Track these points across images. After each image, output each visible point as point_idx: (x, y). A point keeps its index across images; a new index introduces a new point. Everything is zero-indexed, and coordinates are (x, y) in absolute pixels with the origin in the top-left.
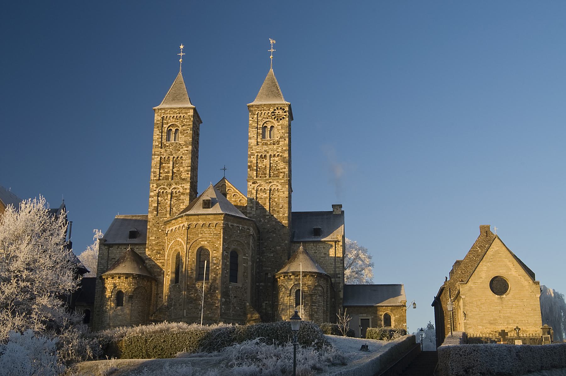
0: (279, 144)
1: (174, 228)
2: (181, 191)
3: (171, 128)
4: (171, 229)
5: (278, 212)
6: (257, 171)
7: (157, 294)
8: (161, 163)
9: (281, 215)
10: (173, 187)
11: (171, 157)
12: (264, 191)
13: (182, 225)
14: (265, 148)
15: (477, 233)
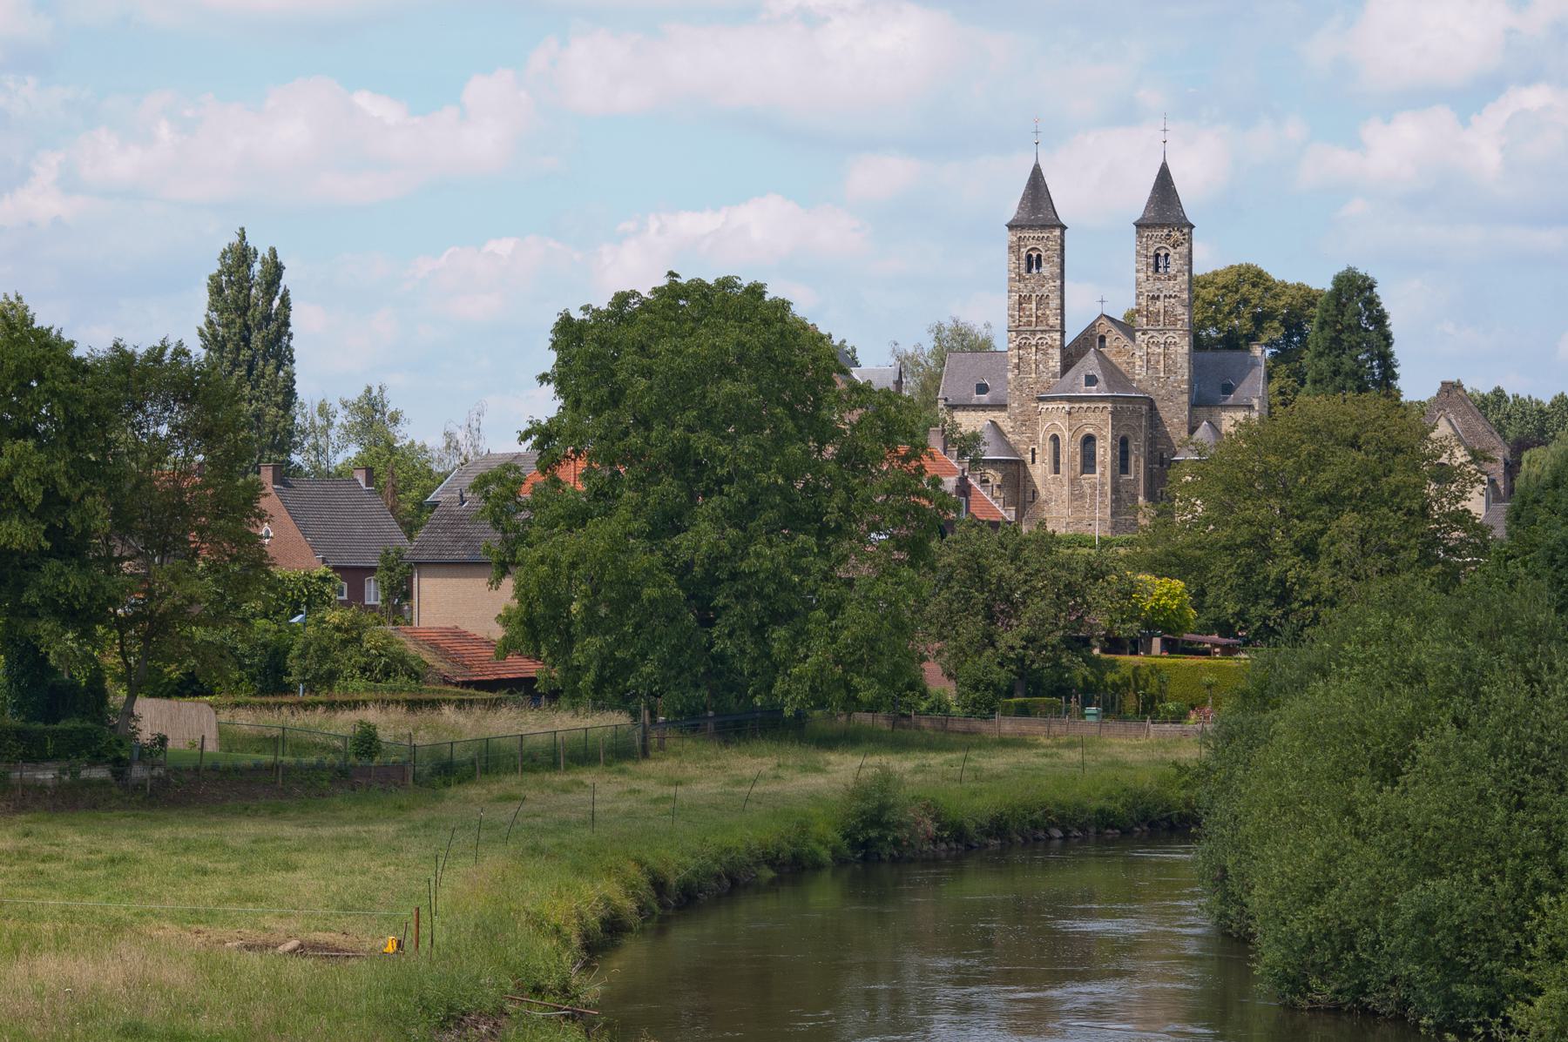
1: (1050, 407)
4: (1045, 407)
6: (1147, 317)
7: (1025, 477)
8: (1020, 304)
9: (1179, 377)
10: (1039, 336)
11: (1034, 295)
13: (1061, 406)
14: (1159, 285)
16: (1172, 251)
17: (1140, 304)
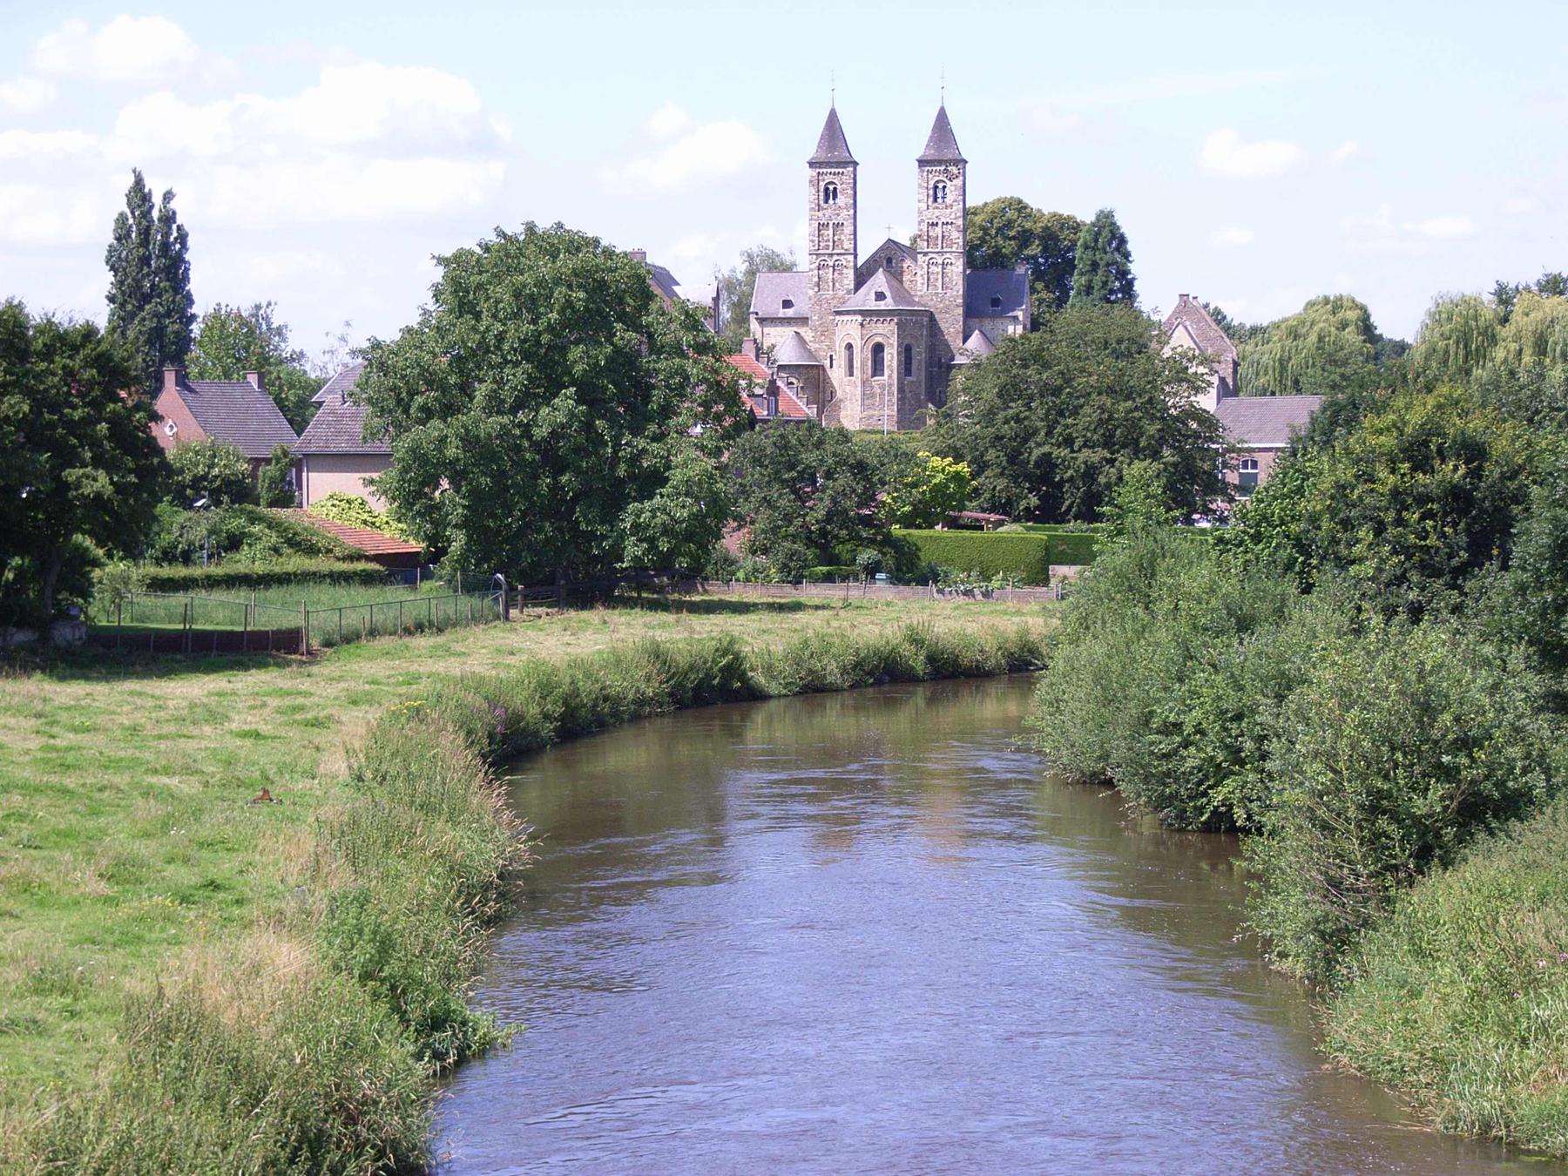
15: (1176, 301)
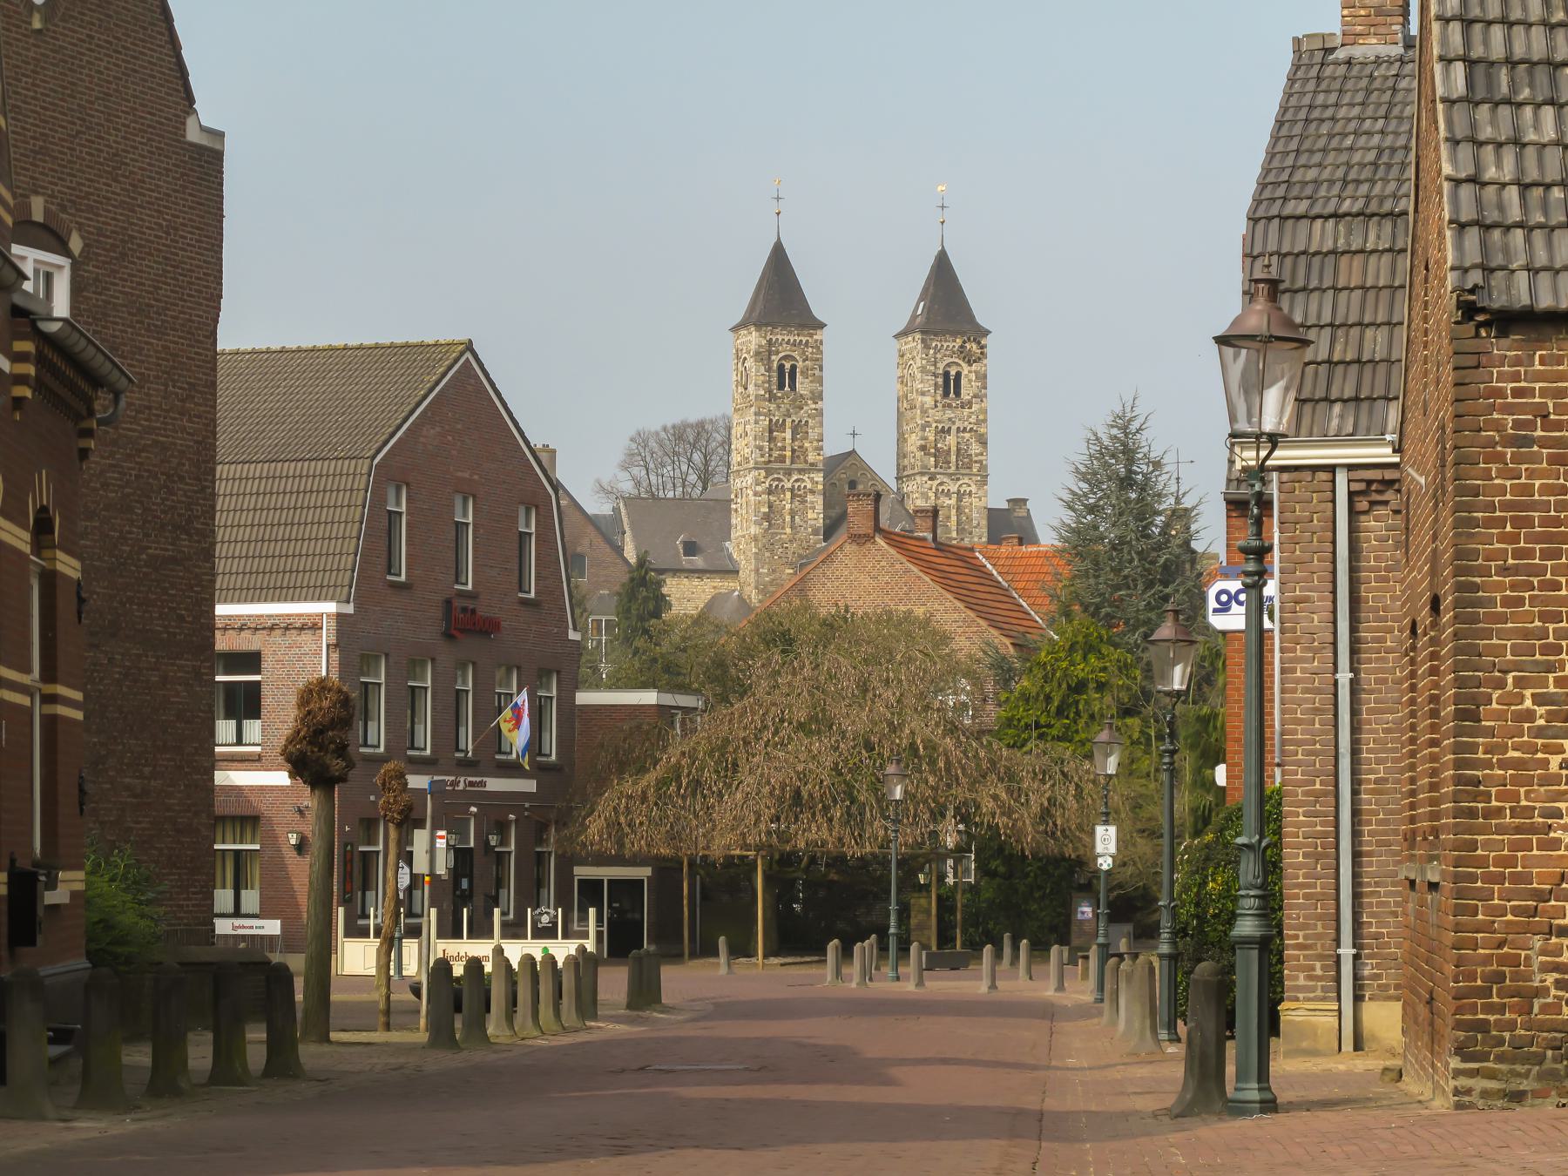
0: (970, 408)
2: (809, 486)
3: (784, 362)
5: (971, 533)
6: (935, 456)
8: (771, 432)
10: (795, 477)
11: (789, 421)
12: (948, 494)
14: (949, 414)
16: (965, 369)
17: (925, 439)
